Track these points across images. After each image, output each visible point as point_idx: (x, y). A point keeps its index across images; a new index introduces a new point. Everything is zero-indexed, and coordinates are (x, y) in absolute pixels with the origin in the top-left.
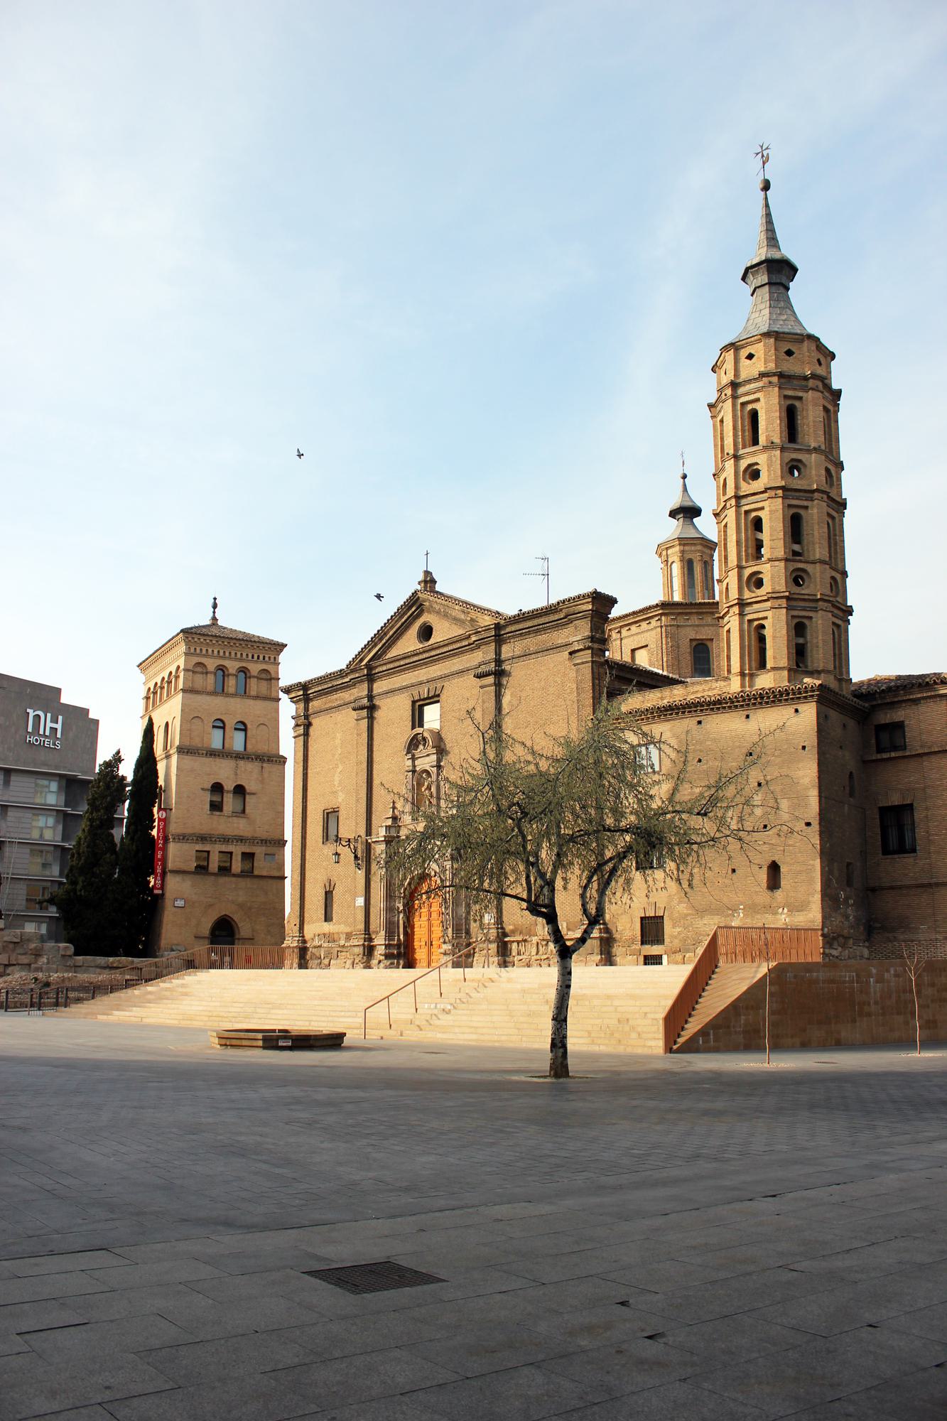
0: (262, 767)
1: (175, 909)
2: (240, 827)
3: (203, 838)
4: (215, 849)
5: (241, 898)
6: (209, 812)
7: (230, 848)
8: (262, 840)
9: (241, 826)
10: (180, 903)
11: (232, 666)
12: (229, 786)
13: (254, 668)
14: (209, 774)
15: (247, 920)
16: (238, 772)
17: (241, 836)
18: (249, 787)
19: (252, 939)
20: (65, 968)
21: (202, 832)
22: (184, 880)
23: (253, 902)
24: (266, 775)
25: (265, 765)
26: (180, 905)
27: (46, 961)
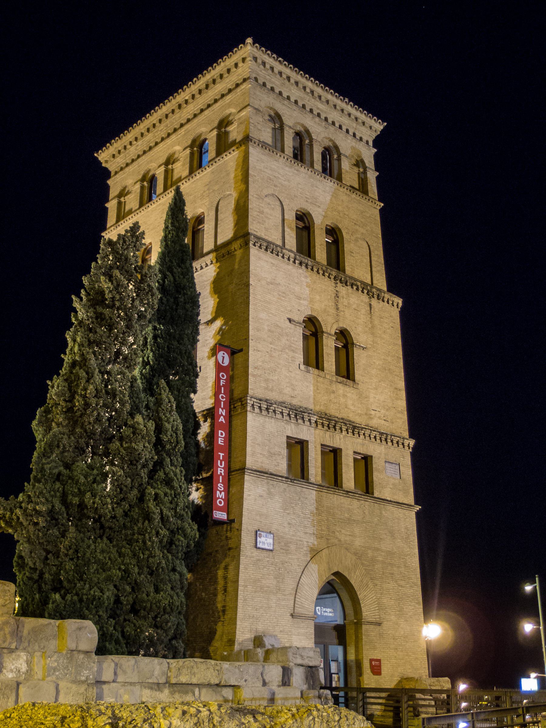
0: (370, 305)
1: (256, 553)
5: (358, 542)
6: (303, 367)
8: (382, 434)
9: (350, 402)
10: (265, 541)
15: (371, 585)
16: (340, 306)
17: (350, 421)
20: (74, 687)
22: (270, 493)
23: (378, 550)
24: (376, 322)
25: (374, 302)
26: (266, 547)
27: (24, 668)
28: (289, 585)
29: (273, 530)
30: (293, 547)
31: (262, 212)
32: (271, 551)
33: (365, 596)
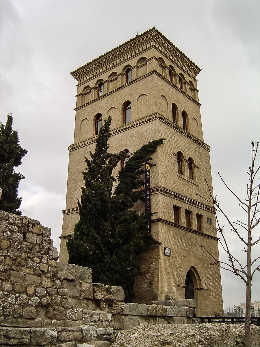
0: (200, 148)
1: (164, 257)
2: (189, 191)
3: (178, 196)
4: (184, 207)
7: (190, 208)
8: (206, 205)
10: (168, 252)
11: (178, 71)
12: (186, 157)
13: (188, 79)
14: (175, 143)
18: (196, 162)
19: (207, 290)
21: (176, 190)
22: (168, 231)
28: (176, 272)
29: (170, 247)
30: (177, 255)
31: (160, 104)
32: (170, 256)
33: (202, 277)
